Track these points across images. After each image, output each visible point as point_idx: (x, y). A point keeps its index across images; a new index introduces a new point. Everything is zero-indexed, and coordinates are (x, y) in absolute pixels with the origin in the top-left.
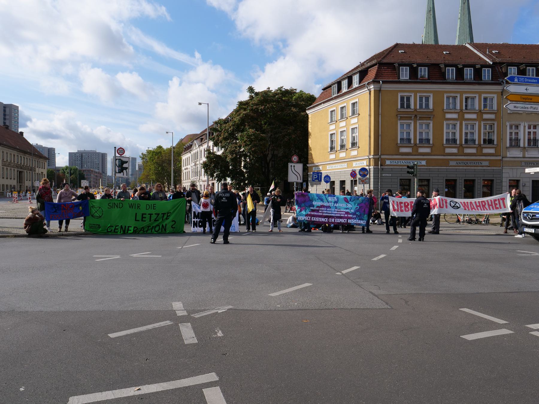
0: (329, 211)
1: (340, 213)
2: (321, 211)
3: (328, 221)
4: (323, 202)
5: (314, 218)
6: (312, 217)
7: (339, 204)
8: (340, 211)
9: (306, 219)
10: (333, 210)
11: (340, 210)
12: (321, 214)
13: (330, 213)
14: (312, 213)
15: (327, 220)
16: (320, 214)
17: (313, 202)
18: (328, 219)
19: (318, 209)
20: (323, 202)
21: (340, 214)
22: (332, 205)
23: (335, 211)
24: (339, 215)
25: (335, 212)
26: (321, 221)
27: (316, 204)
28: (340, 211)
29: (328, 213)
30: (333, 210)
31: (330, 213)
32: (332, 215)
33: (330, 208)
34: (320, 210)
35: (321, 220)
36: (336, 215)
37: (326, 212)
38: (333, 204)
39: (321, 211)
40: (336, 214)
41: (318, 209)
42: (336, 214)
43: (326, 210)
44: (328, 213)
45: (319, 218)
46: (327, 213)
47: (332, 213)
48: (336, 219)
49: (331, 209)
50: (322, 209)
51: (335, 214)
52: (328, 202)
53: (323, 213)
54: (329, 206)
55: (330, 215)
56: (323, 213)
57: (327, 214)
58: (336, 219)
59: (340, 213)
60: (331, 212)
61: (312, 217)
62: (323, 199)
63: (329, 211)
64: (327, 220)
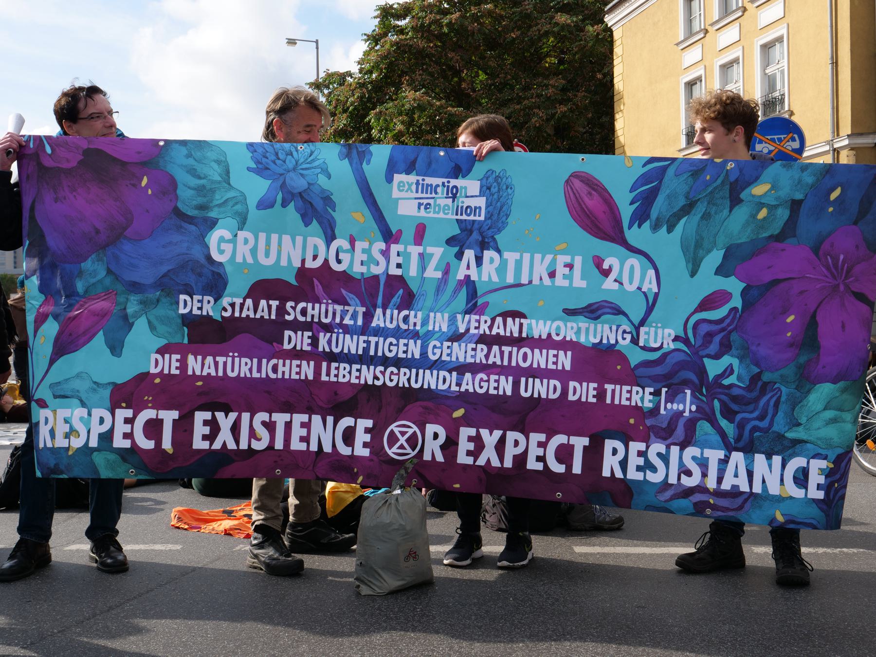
0: (397, 333)
1: (517, 357)
2: (300, 340)
3: (375, 445)
4: (330, 237)
5: (225, 421)
6: (201, 417)
7: (511, 257)
8: (518, 342)
9: (120, 442)
10: (440, 322)
11: (512, 327)
12: (308, 370)
13: (398, 363)
14: (194, 364)
15: (362, 437)
16: (289, 370)
17: (214, 238)
18: (375, 432)
19: (267, 309)
20: (330, 237)
21: (517, 373)
22: (433, 273)
23: (456, 337)
24: (506, 386)
25: (461, 353)
26: (297, 445)
27: (243, 252)
28: (518, 342)
29: (385, 362)
30: (440, 322)
31: (398, 363)
32: (430, 380)
33: (408, 301)
34: (296, 326)
35: (298, 432)
36: (470, 384)
37: (352, 344)
38: (437, 252)
39: (300, 340)
40: (475, 368)
41: (267, 309)
42: (475, 368)
43: (365, 329)
44: (385, 362)
45: (280, 419)
46: (365, 359)
47: (424, 363)
48: (466, 432)
49: (416, 318)
50: (315, 311)
51: (461, 369)
52: (390, 237)
53: (332, 357)
54: (396, 283)
55: (402, 378)
56: (332, 357)
57: (367, 375)
58: (466, 432)
59: (517, 357)
60: (415, 350)
61: (201, 417)
62: (328, 200)
63: (397, 333)
64: (362, 437)
